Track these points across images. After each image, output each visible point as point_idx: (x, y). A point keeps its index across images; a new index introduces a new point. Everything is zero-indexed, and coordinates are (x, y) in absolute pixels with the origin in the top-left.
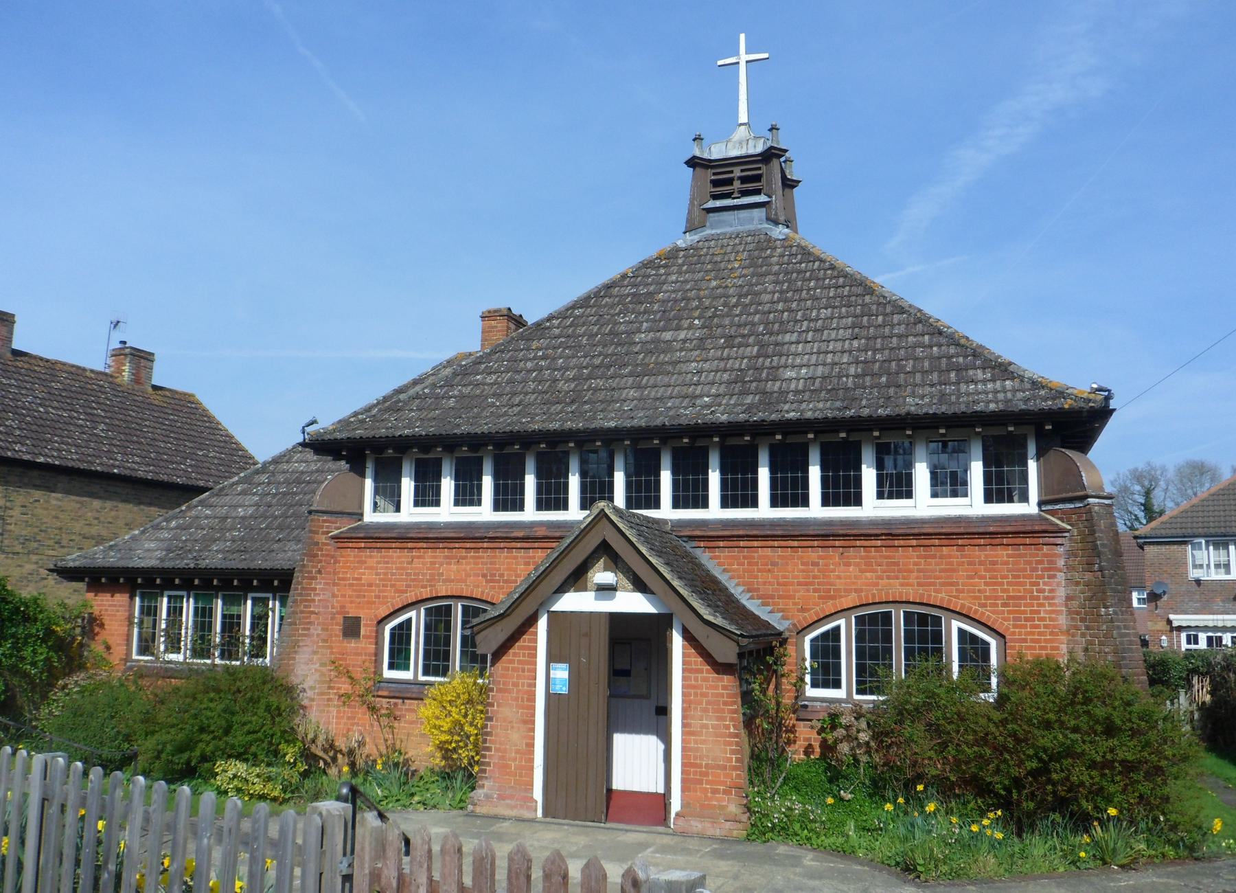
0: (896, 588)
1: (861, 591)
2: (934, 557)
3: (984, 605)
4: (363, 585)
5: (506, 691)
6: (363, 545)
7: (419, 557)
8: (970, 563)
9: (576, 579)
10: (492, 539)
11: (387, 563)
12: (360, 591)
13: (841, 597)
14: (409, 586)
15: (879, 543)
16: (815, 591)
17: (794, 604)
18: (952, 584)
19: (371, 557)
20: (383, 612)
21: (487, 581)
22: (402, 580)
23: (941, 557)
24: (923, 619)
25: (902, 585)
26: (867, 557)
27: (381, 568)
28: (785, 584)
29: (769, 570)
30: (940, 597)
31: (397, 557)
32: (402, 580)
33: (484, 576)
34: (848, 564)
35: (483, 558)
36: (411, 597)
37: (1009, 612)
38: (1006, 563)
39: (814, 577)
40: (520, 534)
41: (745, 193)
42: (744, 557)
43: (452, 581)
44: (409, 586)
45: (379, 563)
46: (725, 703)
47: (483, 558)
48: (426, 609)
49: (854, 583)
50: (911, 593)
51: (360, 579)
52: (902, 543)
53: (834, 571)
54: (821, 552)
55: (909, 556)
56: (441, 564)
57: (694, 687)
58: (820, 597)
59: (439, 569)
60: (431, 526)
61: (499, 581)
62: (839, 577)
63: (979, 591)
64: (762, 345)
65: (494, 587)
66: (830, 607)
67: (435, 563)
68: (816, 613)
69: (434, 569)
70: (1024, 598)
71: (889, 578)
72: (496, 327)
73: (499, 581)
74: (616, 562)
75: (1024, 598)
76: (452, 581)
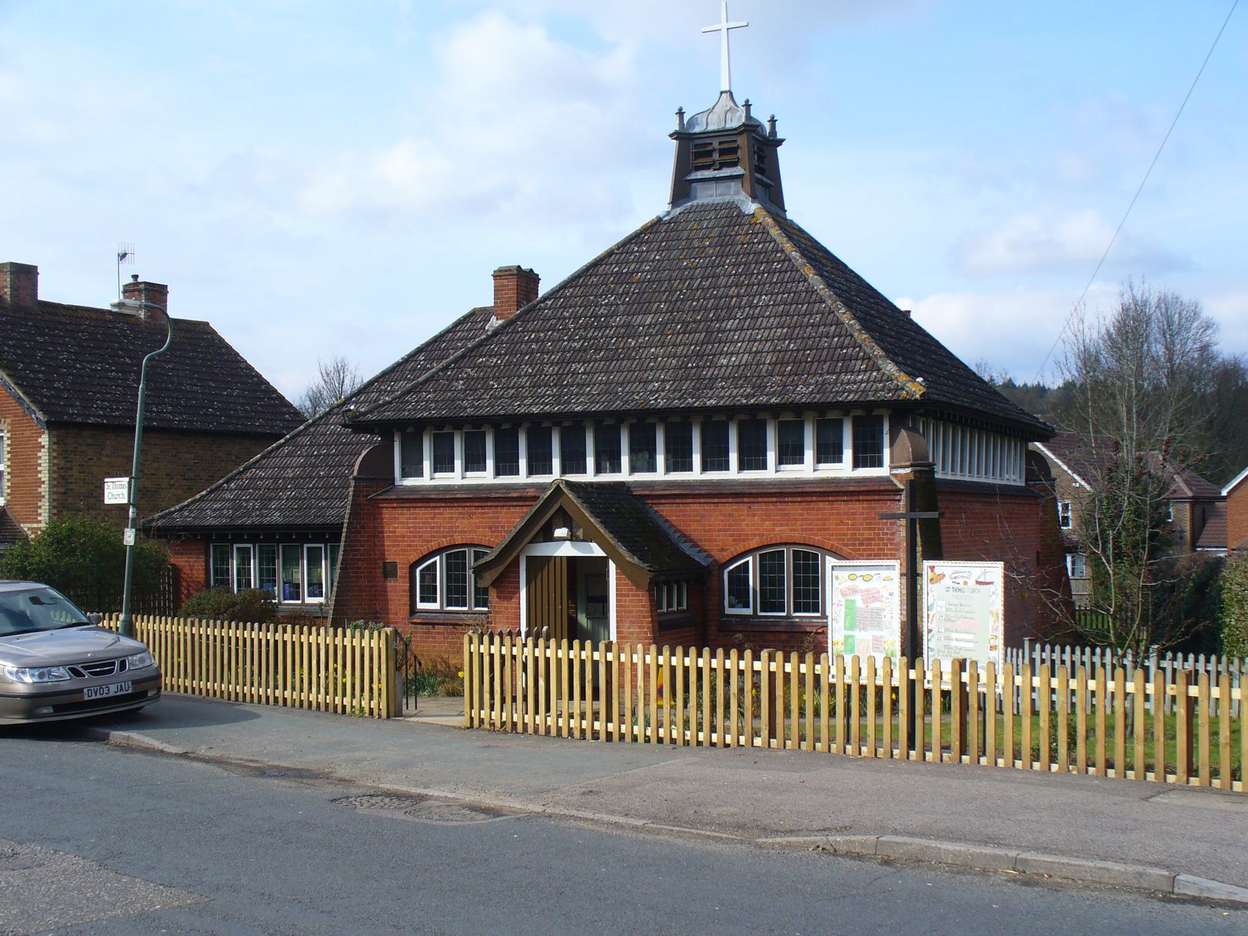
0: (782, 532)
1: (763, 535)
2: (813, 509)
3: (847, 545)
4: (398, 537)
5: (498, 613)
6: (395, 505)
7: (440, 514)
8: (838, 514)
9: (547, 536)
10: (496, 499)
11: (416, 518)
12: (396, 541)
13: (748, 540)
14: (434, 537)
15: (775, 499)
16: (731, 535)
17: (716, 545)
18: (825, 530)
19: (402, 514)
20: (414, 557)
21: (493, 532)
22: (427, 532)
23: (818, 509)
24: (807, 555)
25: (791, 530)
26: (767, 510)
27: (411, 523)
28: (709, 531)
29: (698, 521)
30: (817, 538)
31: (423, 514)
32: (427, 532)
33: (490, 528)
34: (754, 515)
35: (488, 513)
36: (434, 545)
37: (864, 550)
38: (863, 514)
39: (730, 525)
40: (515, 495)
41: (723, 165)
42: (680, 511)
43: (465, 532)
44: (434, 537)
45: (410, 519)
46: (644, 617)
47: (488, 513)
48: (447, 555)
49: (758, 529)
50: (796, 536)
51: (395, 532)
52: (790, 499)
53: (744, 520)
54: (735, 507)
55: (795, 509)
56: (457, 519)
57: (624, 606)
58: (734, 540)
59: (455, 523)
60: (448, 489)
61: (501, 532)
62: (747, 525)
63: (844, 535)
64: (709, 332)
65: (497, 536)
66: (741, 548)
67: (452, 518)
68: (732, 553)
69: (451, 523)
70: (873, 539)
71: (781, 525)
72: (507, 286)
73: (501, 532)
74: (567, 522)
75: (873, 539)
76: (465, 532)
